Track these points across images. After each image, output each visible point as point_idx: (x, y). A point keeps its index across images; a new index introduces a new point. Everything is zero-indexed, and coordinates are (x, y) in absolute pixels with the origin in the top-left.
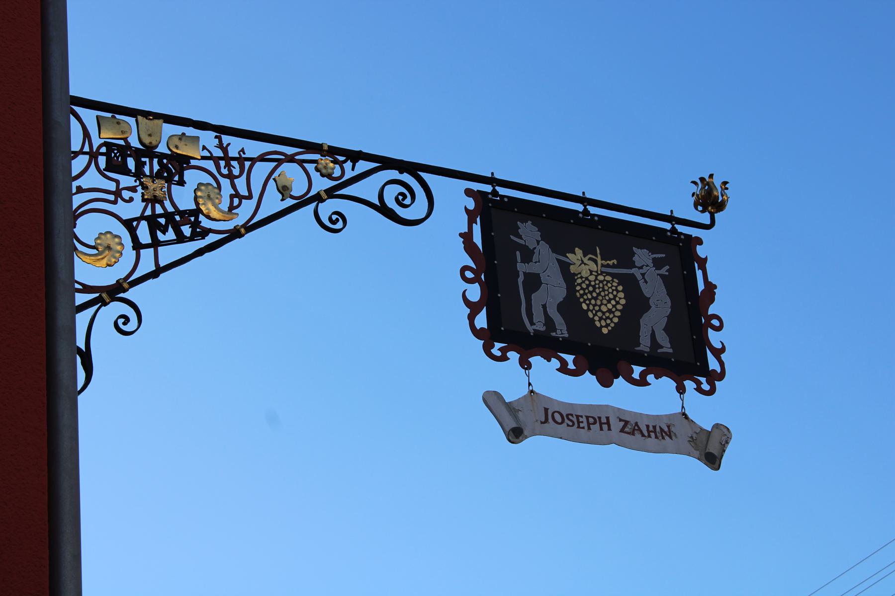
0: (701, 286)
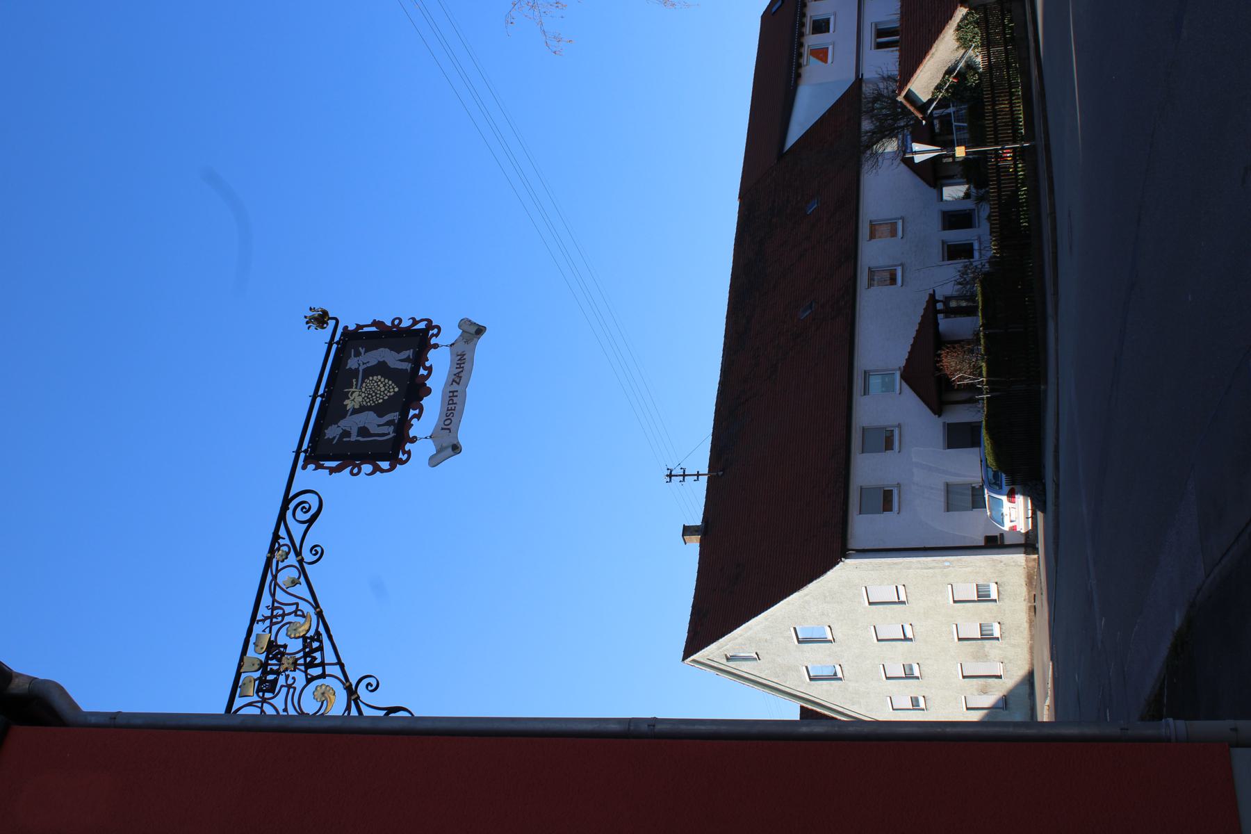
0: (374, 329)
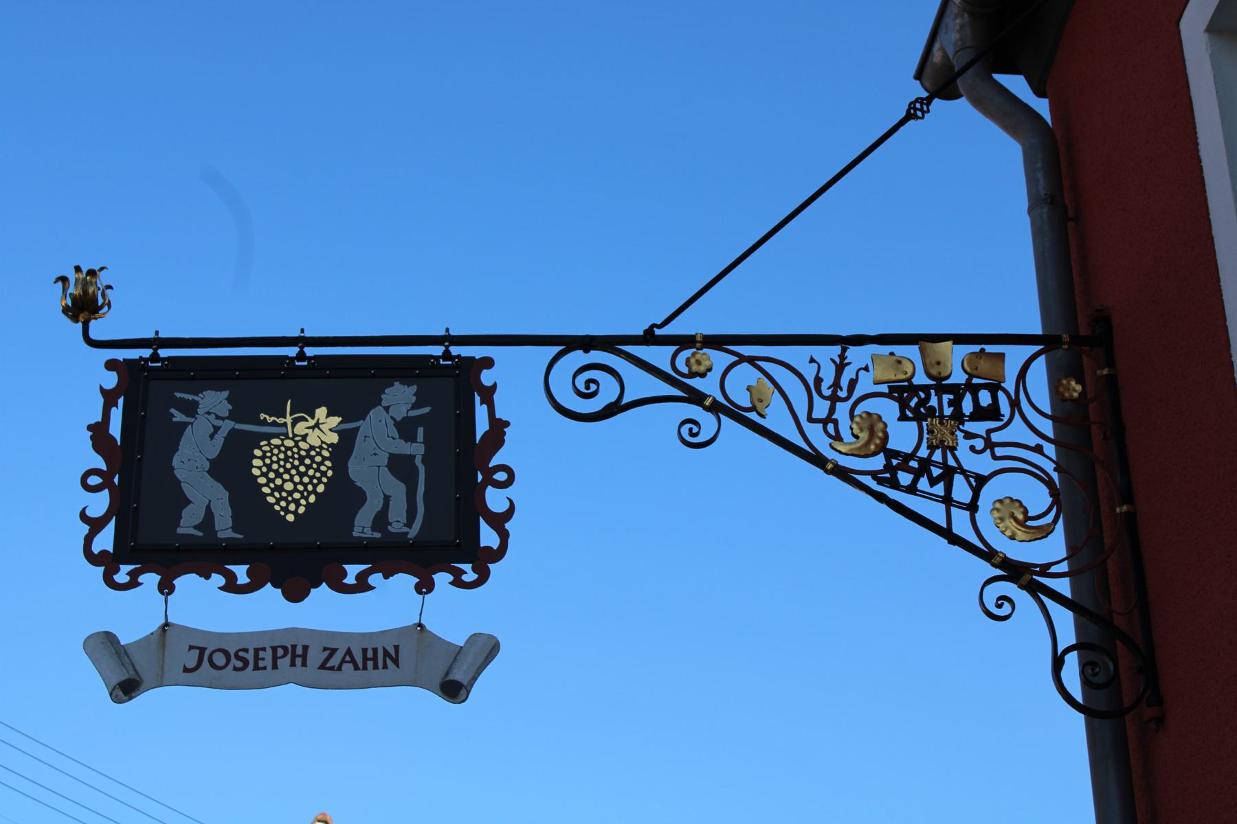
0: (482, 425)
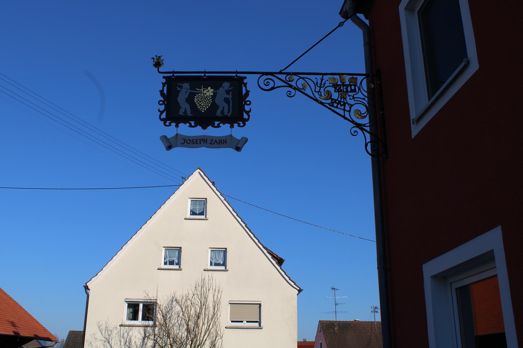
0: (244, 92)
